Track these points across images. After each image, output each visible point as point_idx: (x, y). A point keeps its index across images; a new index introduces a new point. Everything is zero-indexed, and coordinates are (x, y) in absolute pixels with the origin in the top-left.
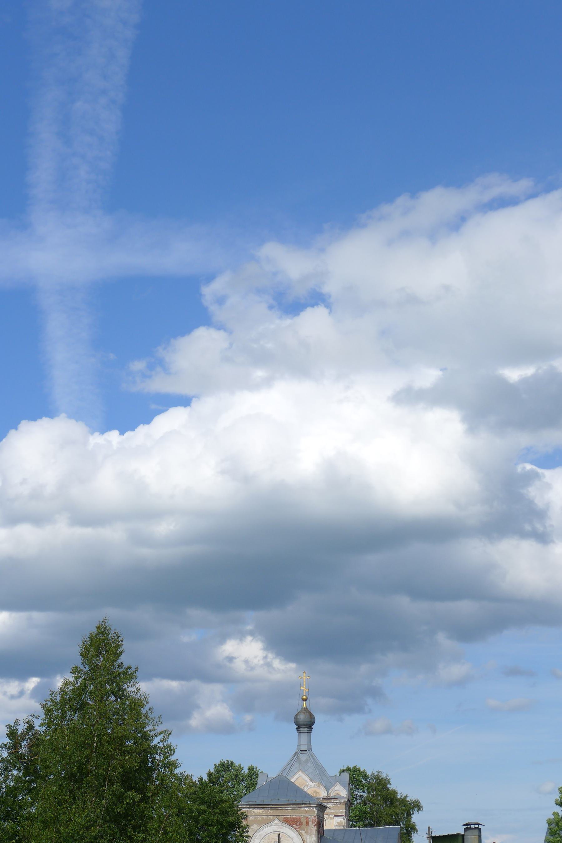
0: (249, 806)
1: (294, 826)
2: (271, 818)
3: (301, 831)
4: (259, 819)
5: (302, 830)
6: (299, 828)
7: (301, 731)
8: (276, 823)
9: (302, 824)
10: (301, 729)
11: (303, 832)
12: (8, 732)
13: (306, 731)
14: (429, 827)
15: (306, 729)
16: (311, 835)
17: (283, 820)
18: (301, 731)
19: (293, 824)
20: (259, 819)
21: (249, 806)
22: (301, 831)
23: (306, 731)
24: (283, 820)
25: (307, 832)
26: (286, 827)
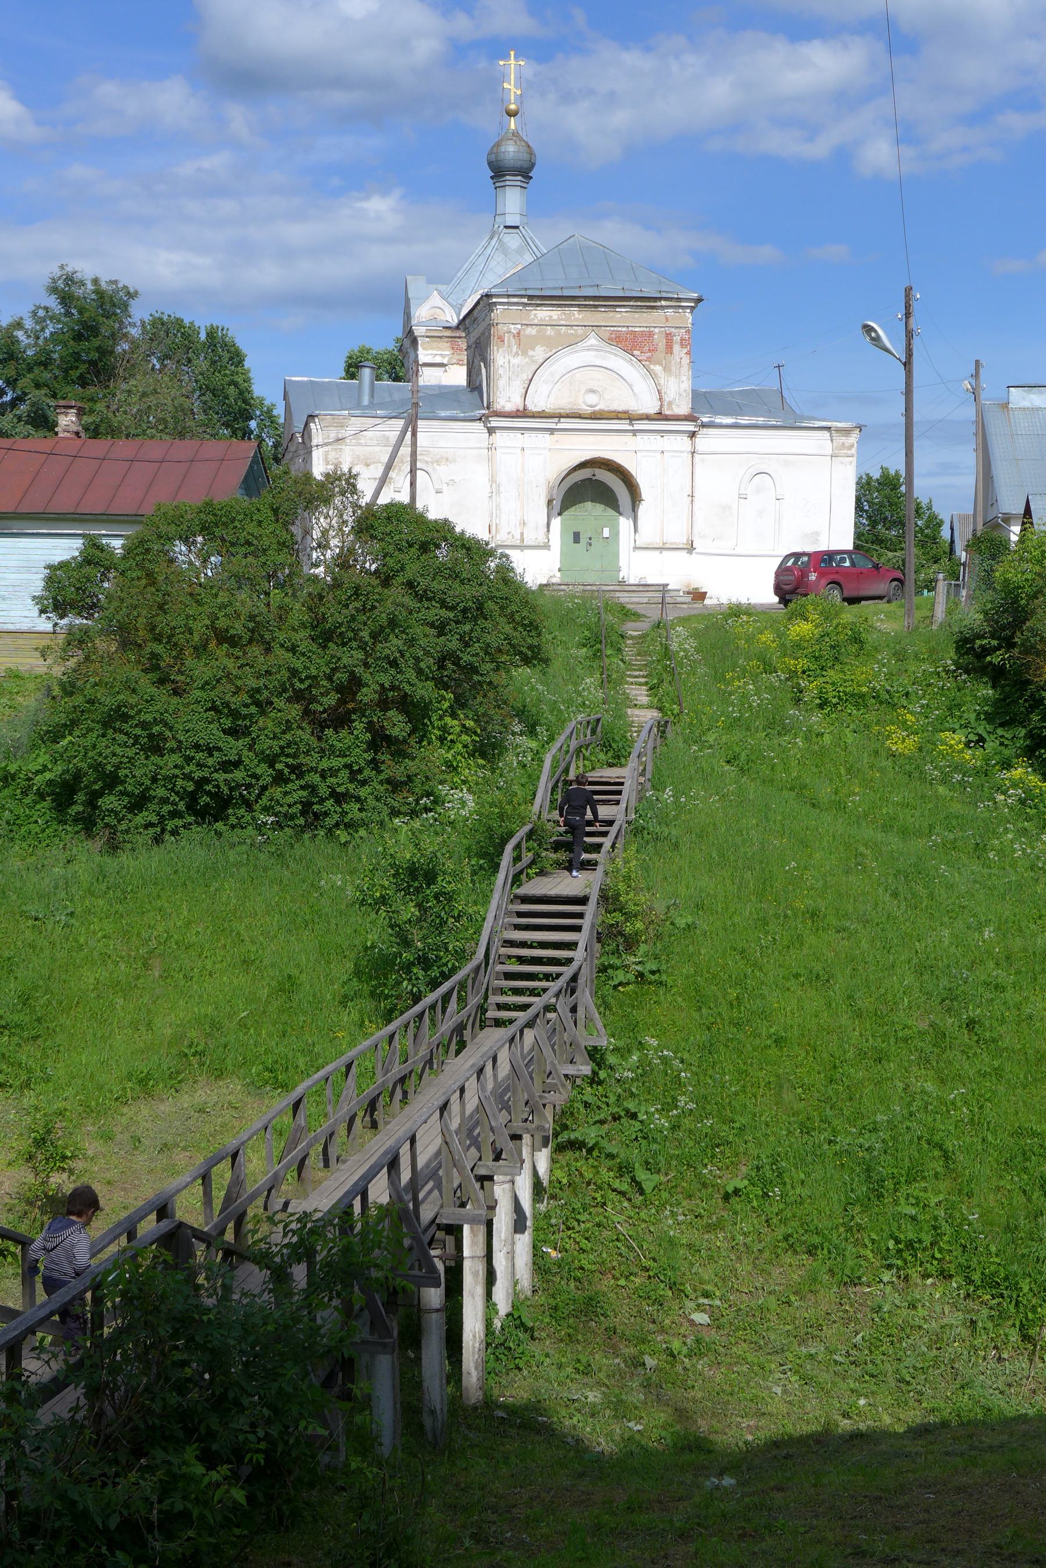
0: (525, 300)
1: (636, 353)
2: (580, 331)
3: (652, 367)
4: (548, 333)
5: (655, 364)
6: (649, 359)
7: (508, 183)
8: (592, 345)
9: (655, 350)
10: (508, 178)
11: (658, 369)
12: (198, 1453)
13: (519, 183)
14: (977, 362)
15: (519, 178)
16: (678, 375)
17: (611, 339)
18: (508, 183)
19: (634, 348)
20: (548, 333)
21: (525, 300)
22: (652, 367)
23: (519, 183)
24: (611, 339)
25: (667, 369)
26: (616, 355)
